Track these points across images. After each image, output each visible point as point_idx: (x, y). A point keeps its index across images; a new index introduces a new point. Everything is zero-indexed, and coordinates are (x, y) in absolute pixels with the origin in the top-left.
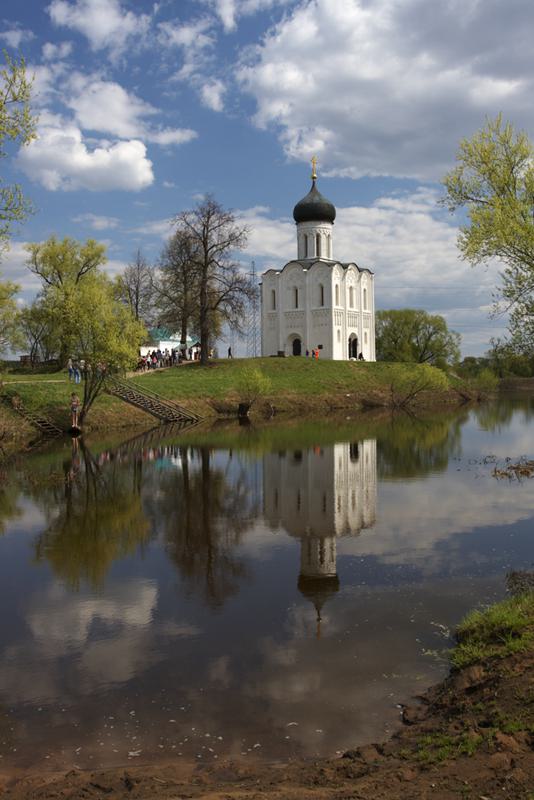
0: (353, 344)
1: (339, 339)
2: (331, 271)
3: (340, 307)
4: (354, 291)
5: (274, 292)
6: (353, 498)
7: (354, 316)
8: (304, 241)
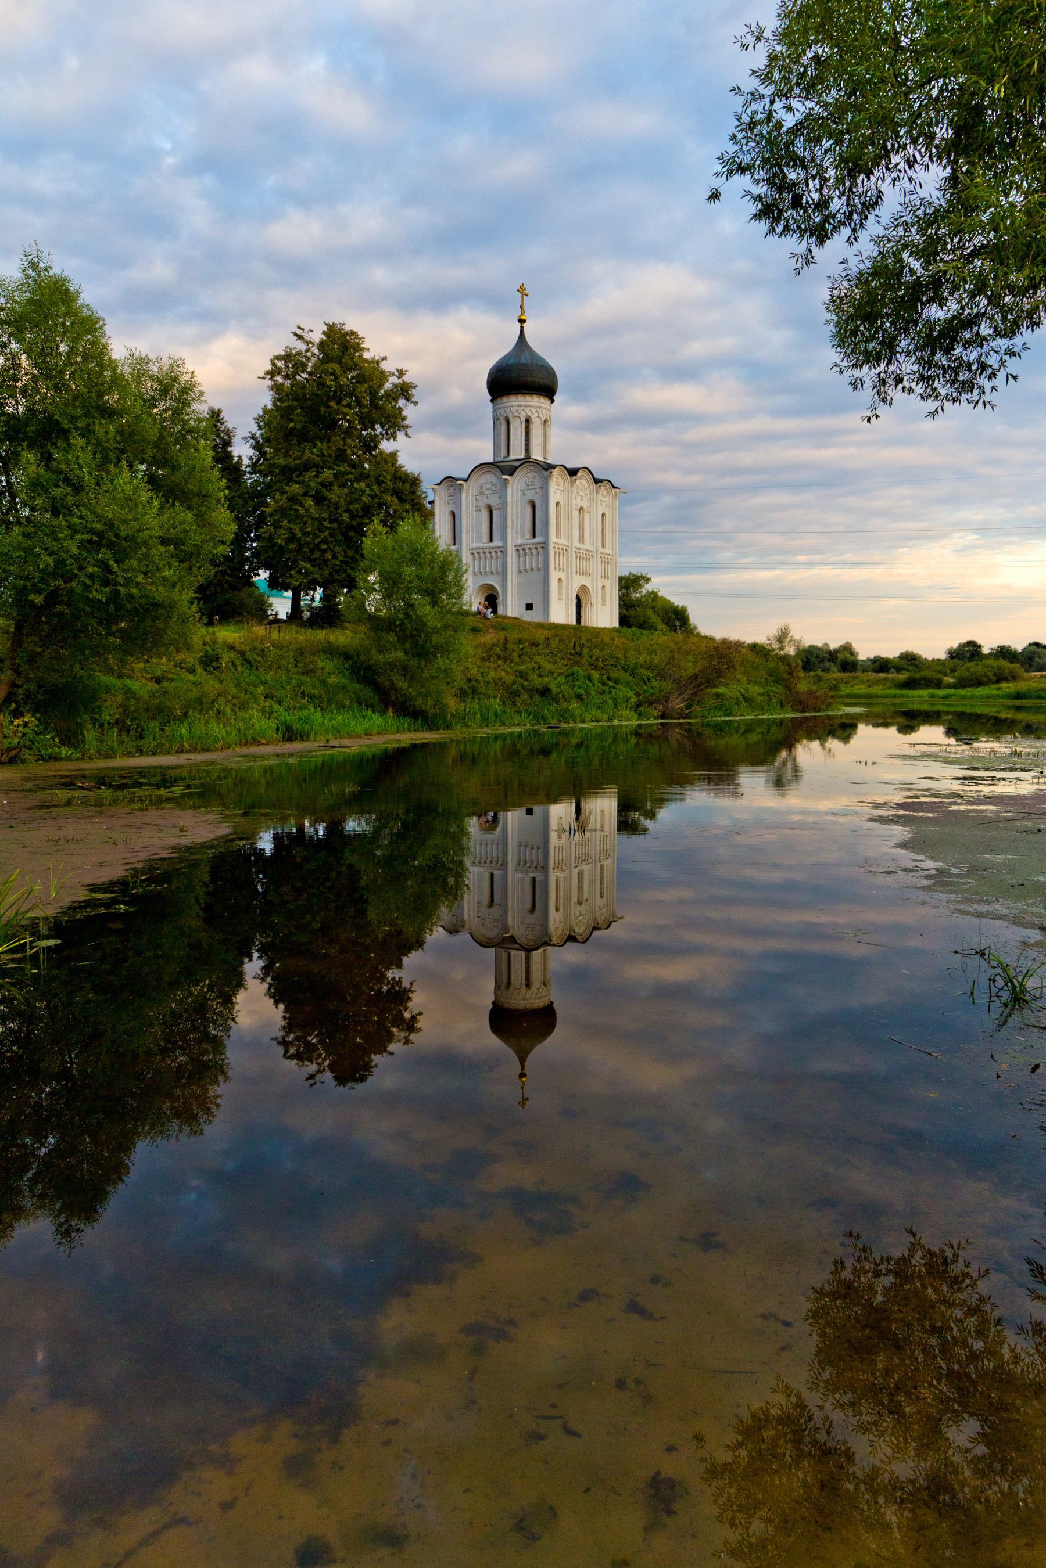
1: (560, 599)
3: (563, 541)
4: (587, 516)
5: (453, 514)
6: (580, 887)
7: (586, 557)
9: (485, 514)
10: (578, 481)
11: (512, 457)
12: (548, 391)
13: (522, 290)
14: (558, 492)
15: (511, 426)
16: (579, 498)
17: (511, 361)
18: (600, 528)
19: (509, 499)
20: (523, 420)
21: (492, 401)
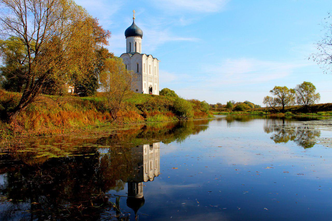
0: (151, 90)
1: (145, 88)
3: (145, 73)
4: (151, 67)
11: (132, 52)
12: (141, 36)
15: (131, 44)
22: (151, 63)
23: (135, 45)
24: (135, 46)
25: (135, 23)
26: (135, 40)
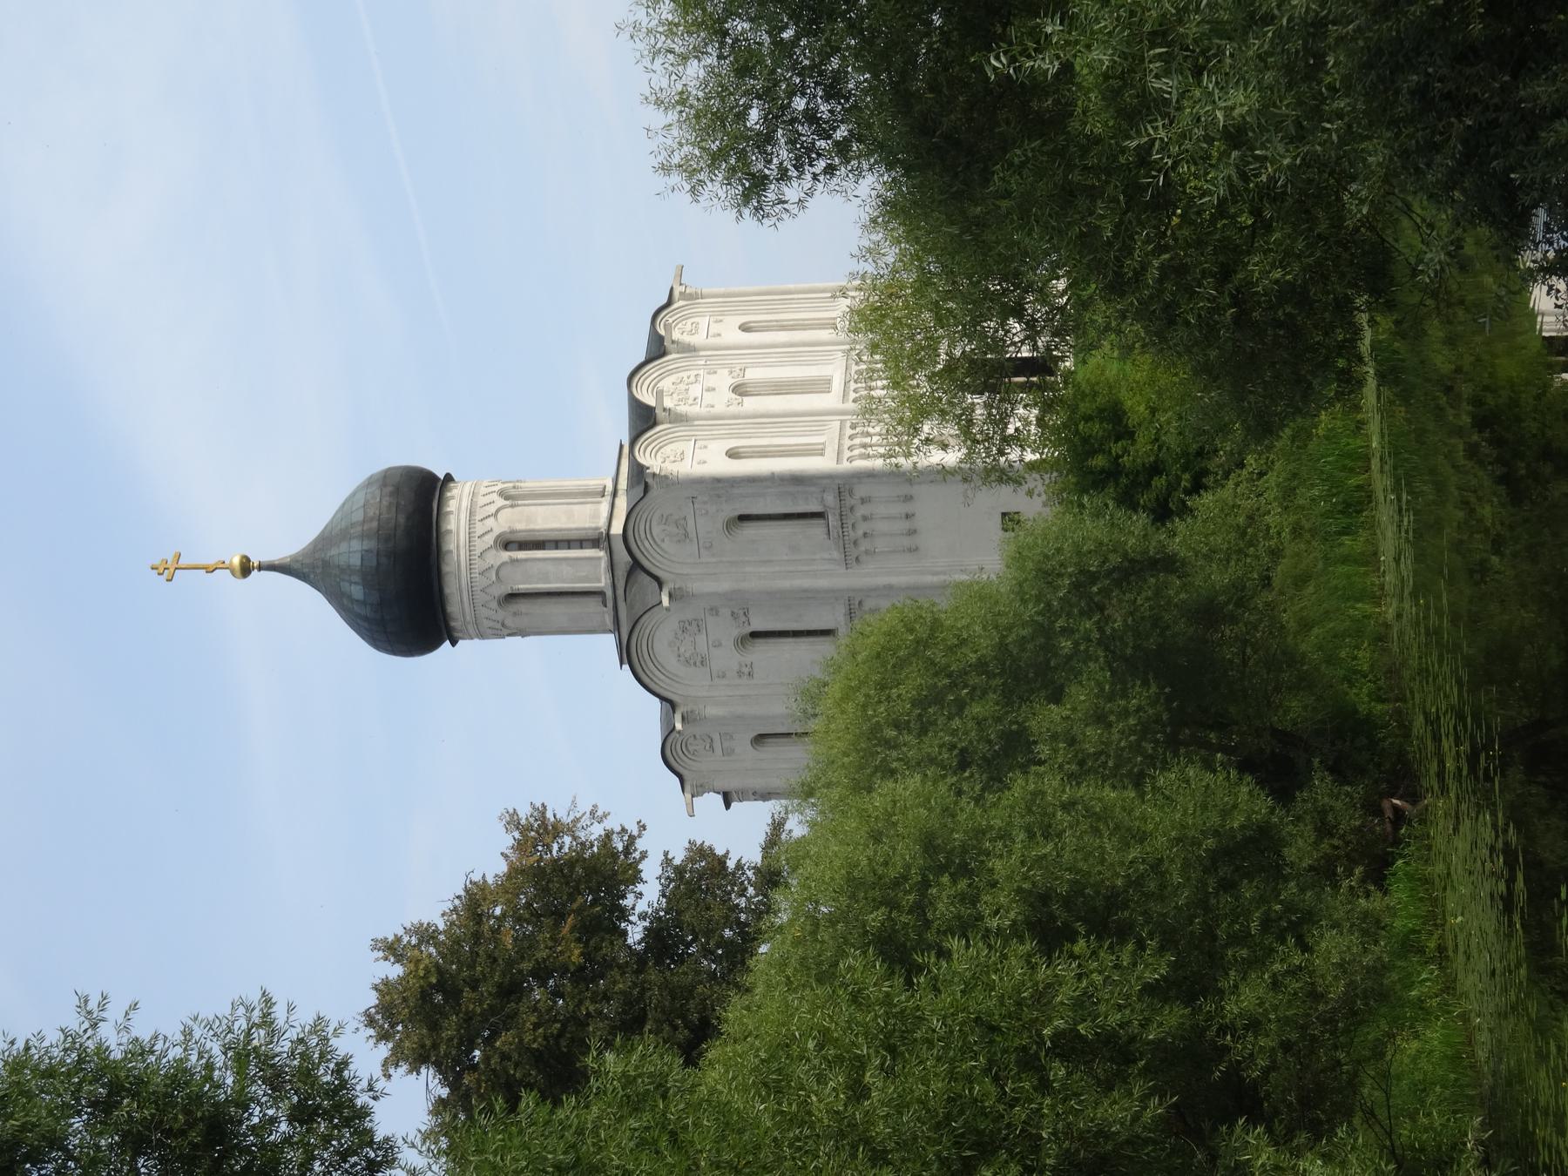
2: (664, 480)
3: (829, 435)
4: (753, 374)
5: (760, 739)
8: (522, 610)
9: (764, 652)
10: (668, 403)
11: (603, 582)
13: (168, 569)
14: (700, 454)
16: (708, 398)
17: (357, 592)
18: (783, 336)
19: (725, 586)
20: (506, 555)
21: (454, 643)
22: (711, 381)
23: (524, 545)
24: (539, 545)
25: (293, 541)
26: (480, 546)
